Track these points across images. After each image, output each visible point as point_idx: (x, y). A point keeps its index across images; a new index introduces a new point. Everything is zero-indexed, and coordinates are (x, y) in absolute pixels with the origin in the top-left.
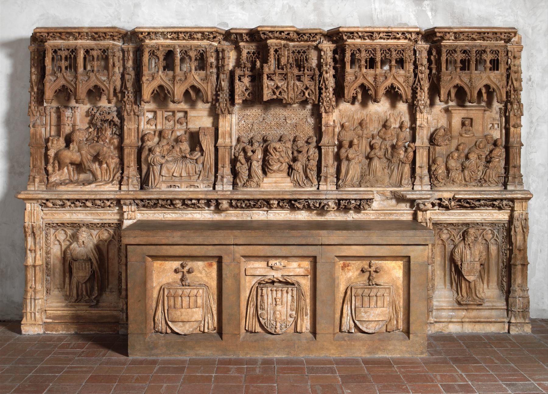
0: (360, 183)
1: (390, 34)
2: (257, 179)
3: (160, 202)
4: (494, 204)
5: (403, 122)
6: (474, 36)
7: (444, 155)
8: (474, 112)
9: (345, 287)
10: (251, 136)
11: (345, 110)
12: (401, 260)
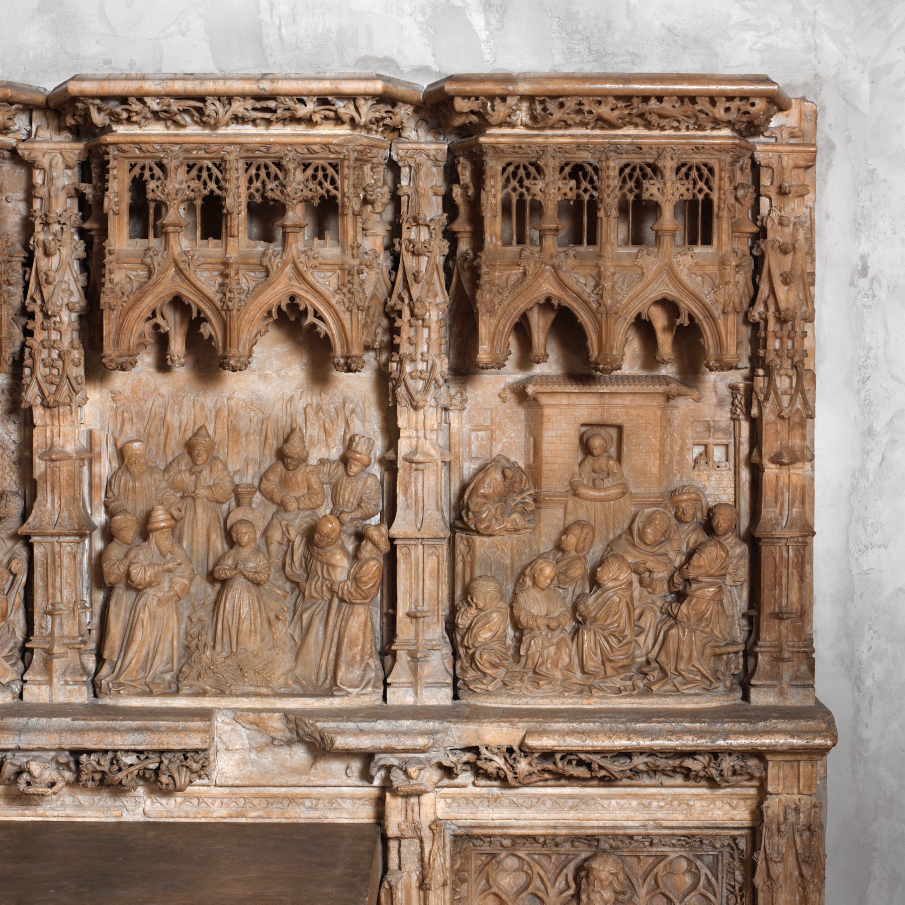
0: (178, 679)
1: (272, 104)
6: (604, 110)
7: (505, 568)
8: (627, 401)
11: (133, 391)
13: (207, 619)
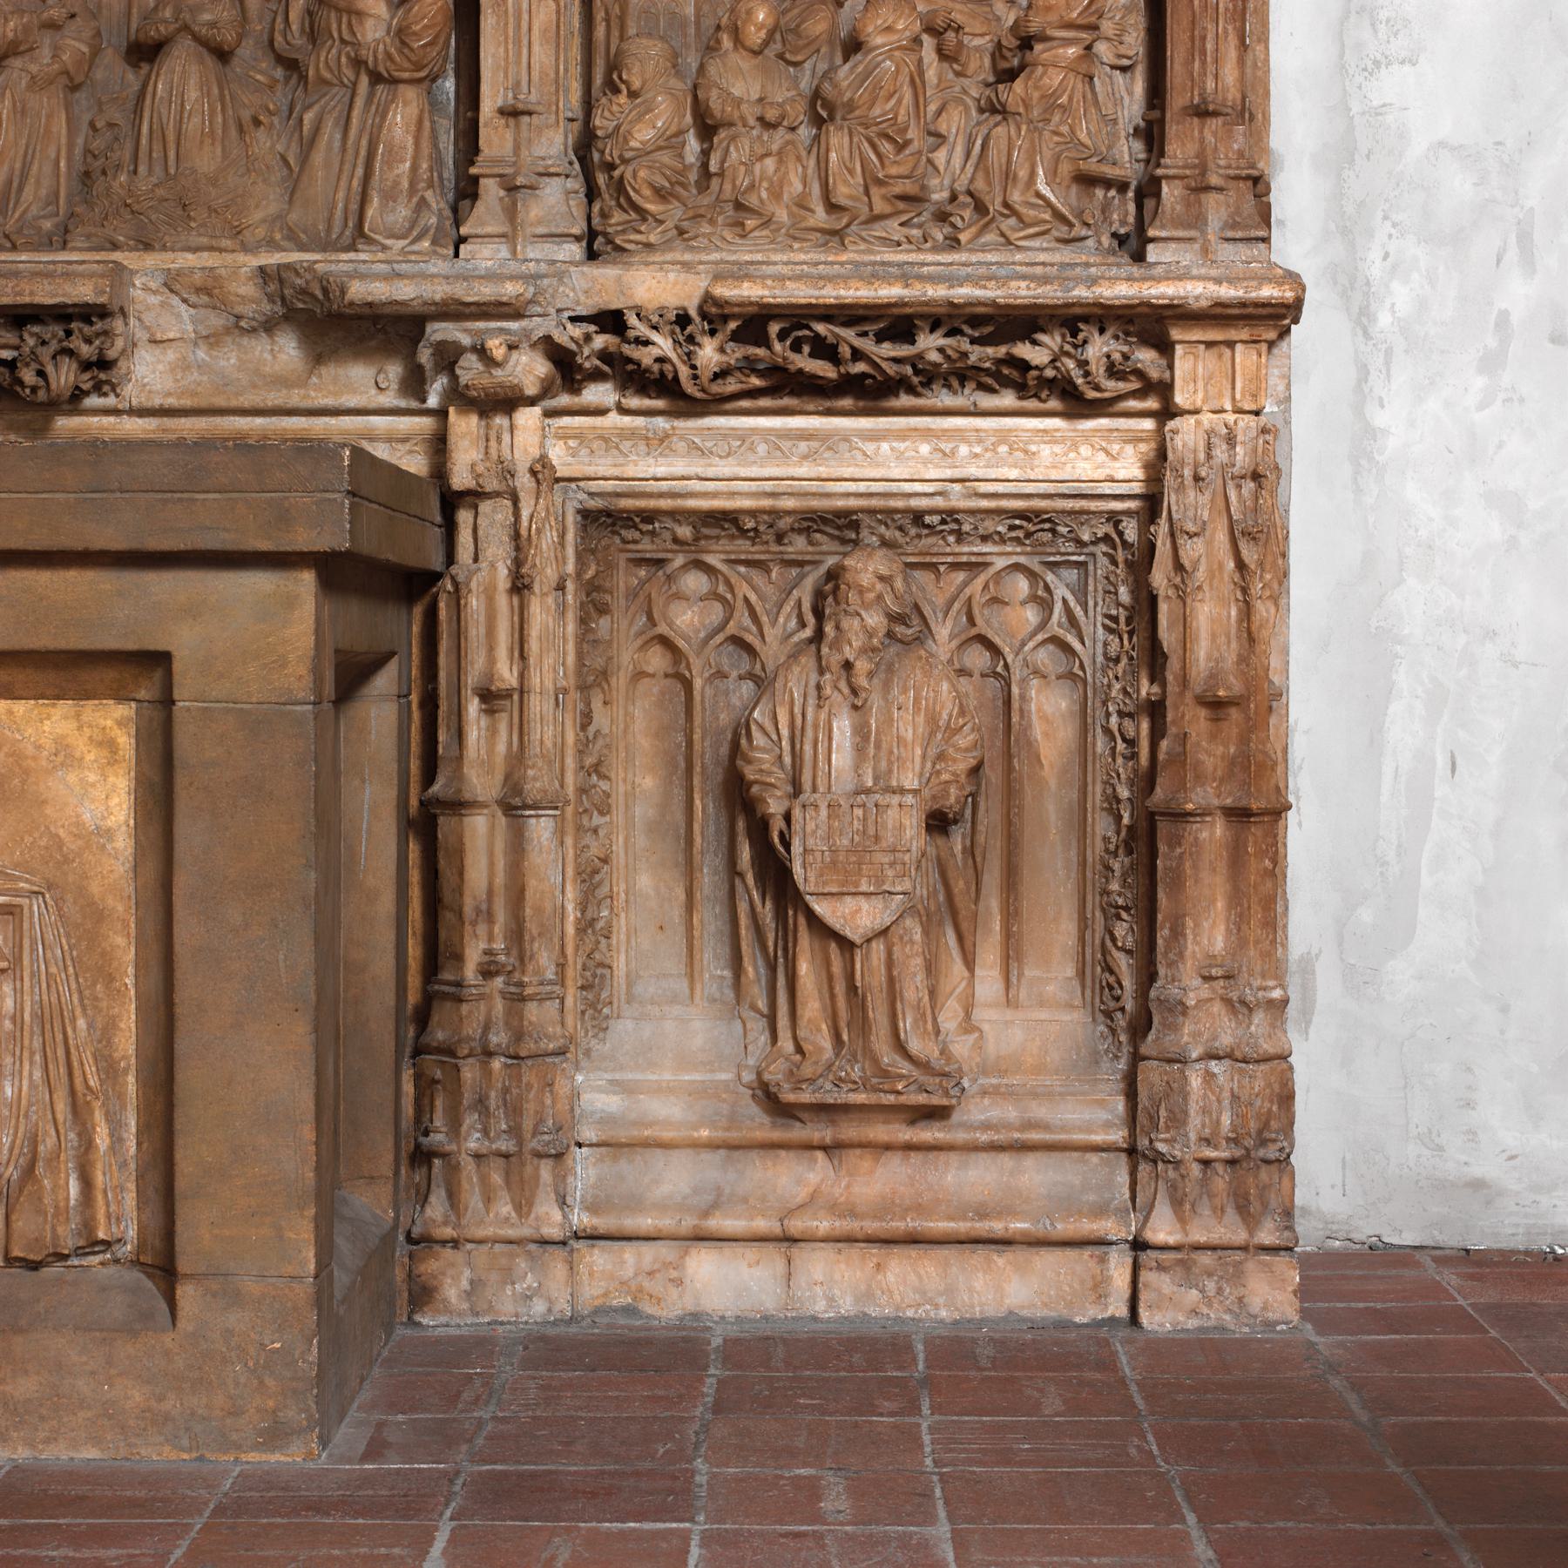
4: (1024, 366)
7: (683, 24)
12: (120, 698)
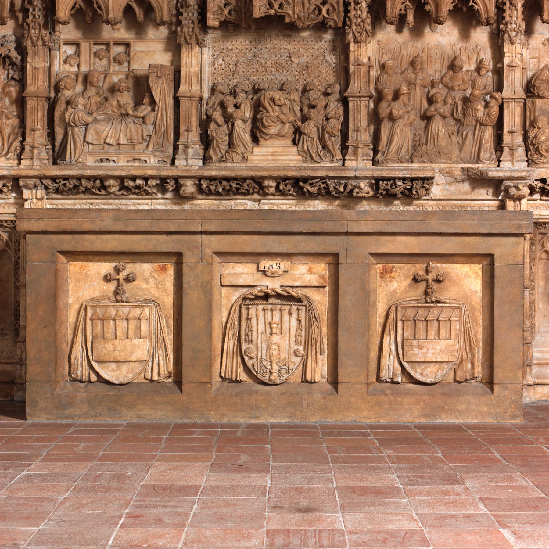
0: (411, 158)
2: (242, 148)
3: (84, 182)
5: (481, 61)
9: (386, 307)
10: (234, 84)
11: (387, 41)
12: (479, 263)
13: (423, 135)
